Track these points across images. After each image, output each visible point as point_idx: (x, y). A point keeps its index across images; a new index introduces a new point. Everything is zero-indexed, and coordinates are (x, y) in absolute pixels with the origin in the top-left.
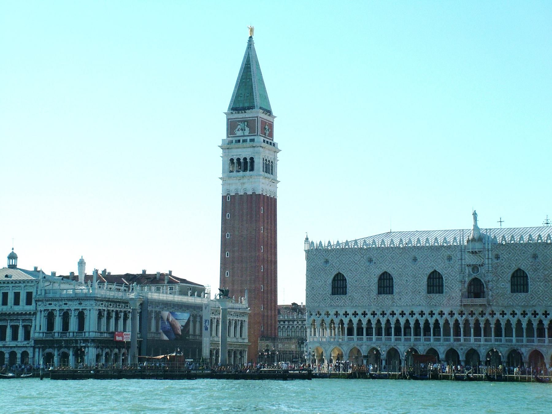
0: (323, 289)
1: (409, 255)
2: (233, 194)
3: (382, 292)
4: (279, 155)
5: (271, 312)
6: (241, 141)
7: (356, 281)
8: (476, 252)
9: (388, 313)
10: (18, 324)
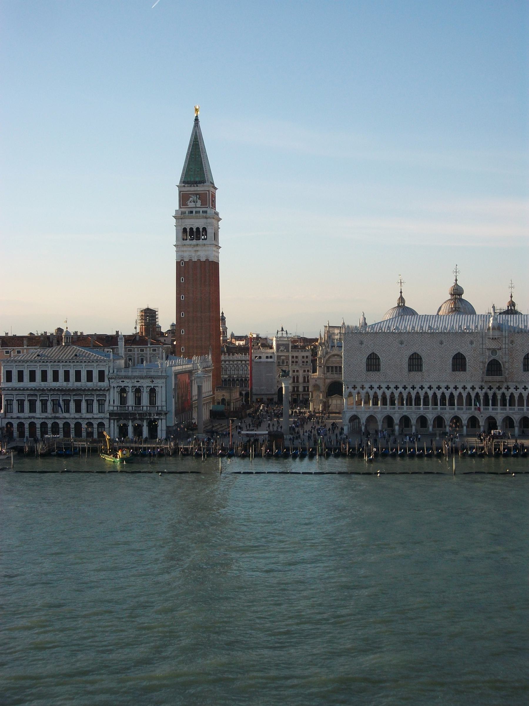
0: (359, 366)
1: (436, 339)
3: (412, 370)
6: (194, 212)
7: (389, 360)
8: (495, 338)
9: (418, 386)
10: (93, 398)
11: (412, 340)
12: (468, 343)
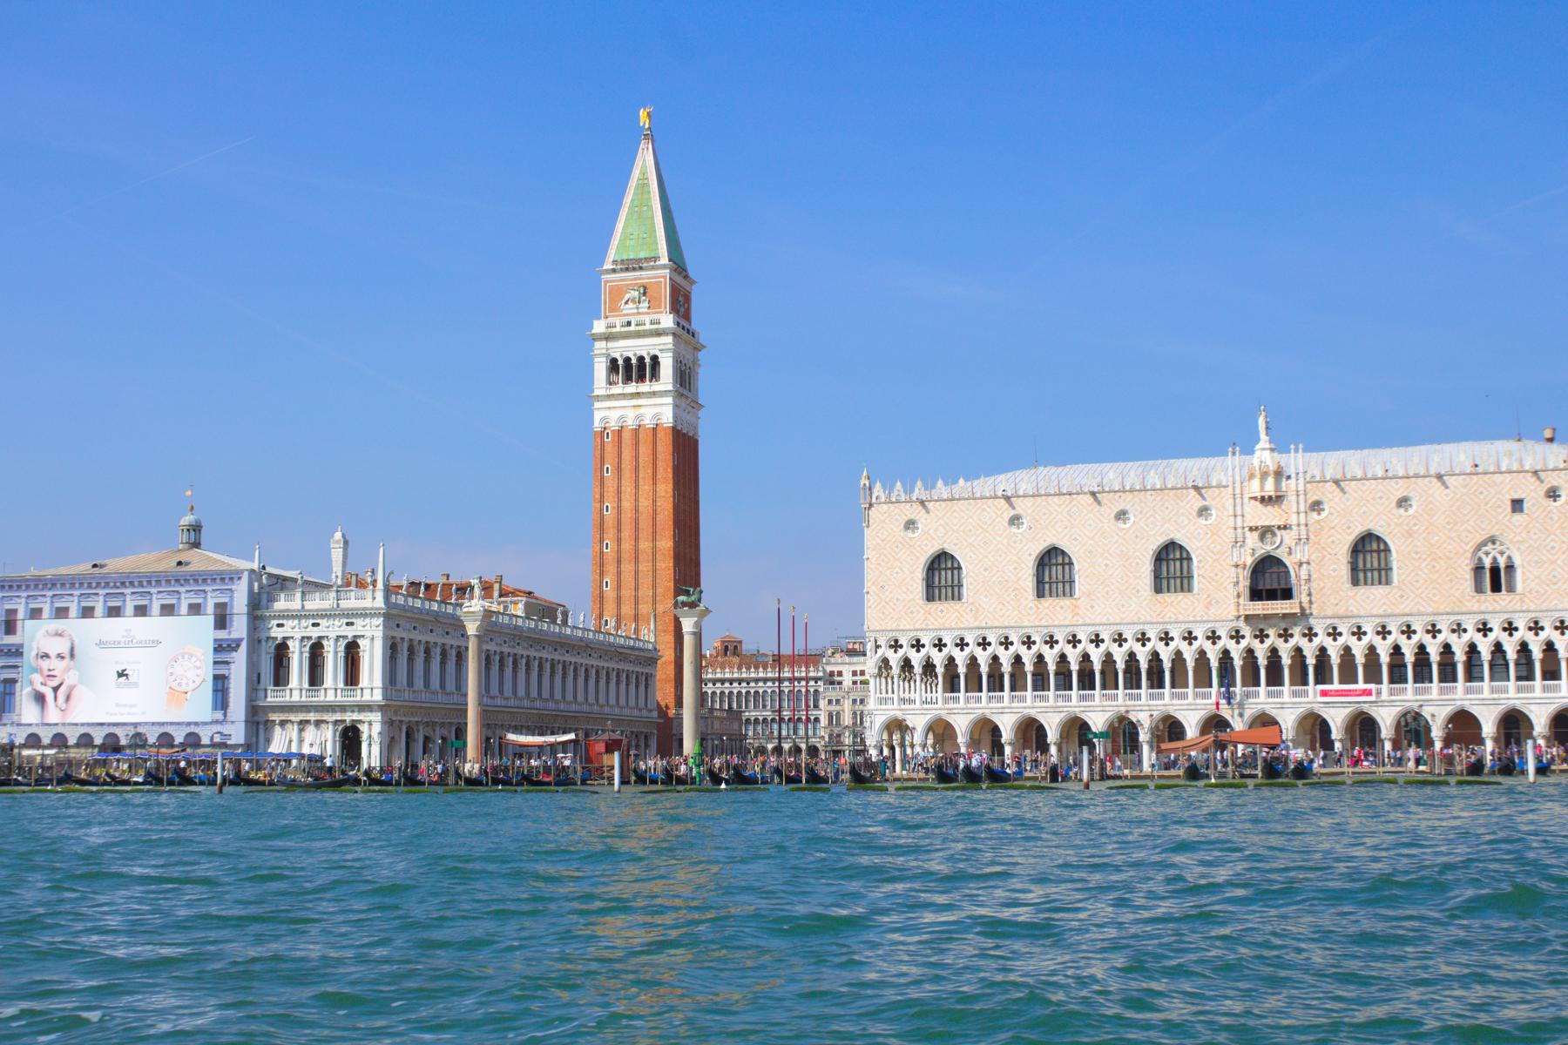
2: (613, 425)
4: (701, 355)
6: (633, 324)
7: (986, 570)
8: (1270, 497)
11: (1045, 514)
12: (1195, 514)
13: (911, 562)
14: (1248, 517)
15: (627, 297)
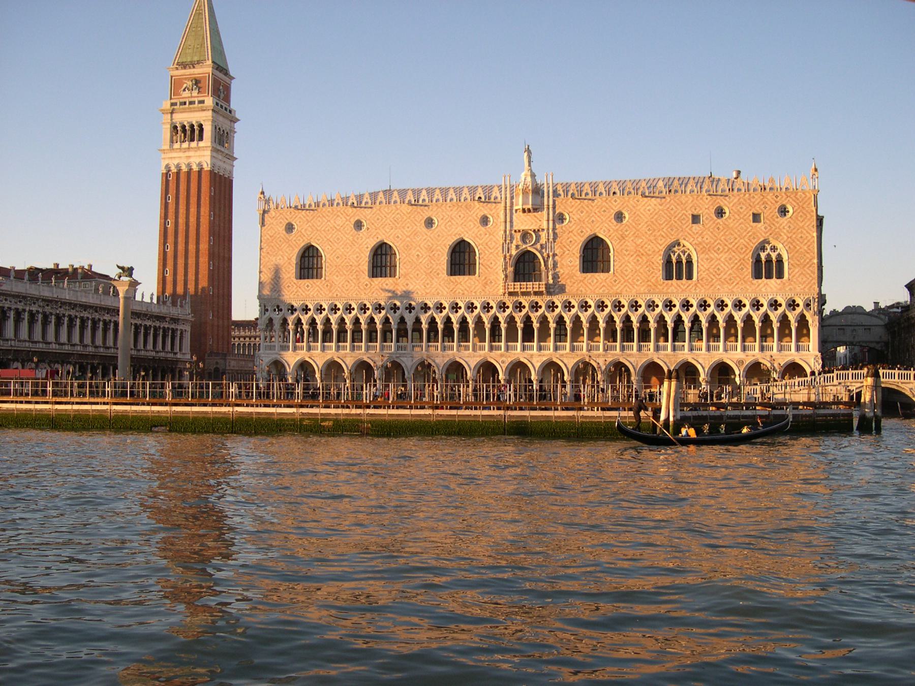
4: (237, 125)
5: (223, 322)
6: (187, 103)
7: (338, 257)
8: (529, 211)
11: (378, 219)
13: (289, 252)
14: (515, 224)
15: (185, 85)
